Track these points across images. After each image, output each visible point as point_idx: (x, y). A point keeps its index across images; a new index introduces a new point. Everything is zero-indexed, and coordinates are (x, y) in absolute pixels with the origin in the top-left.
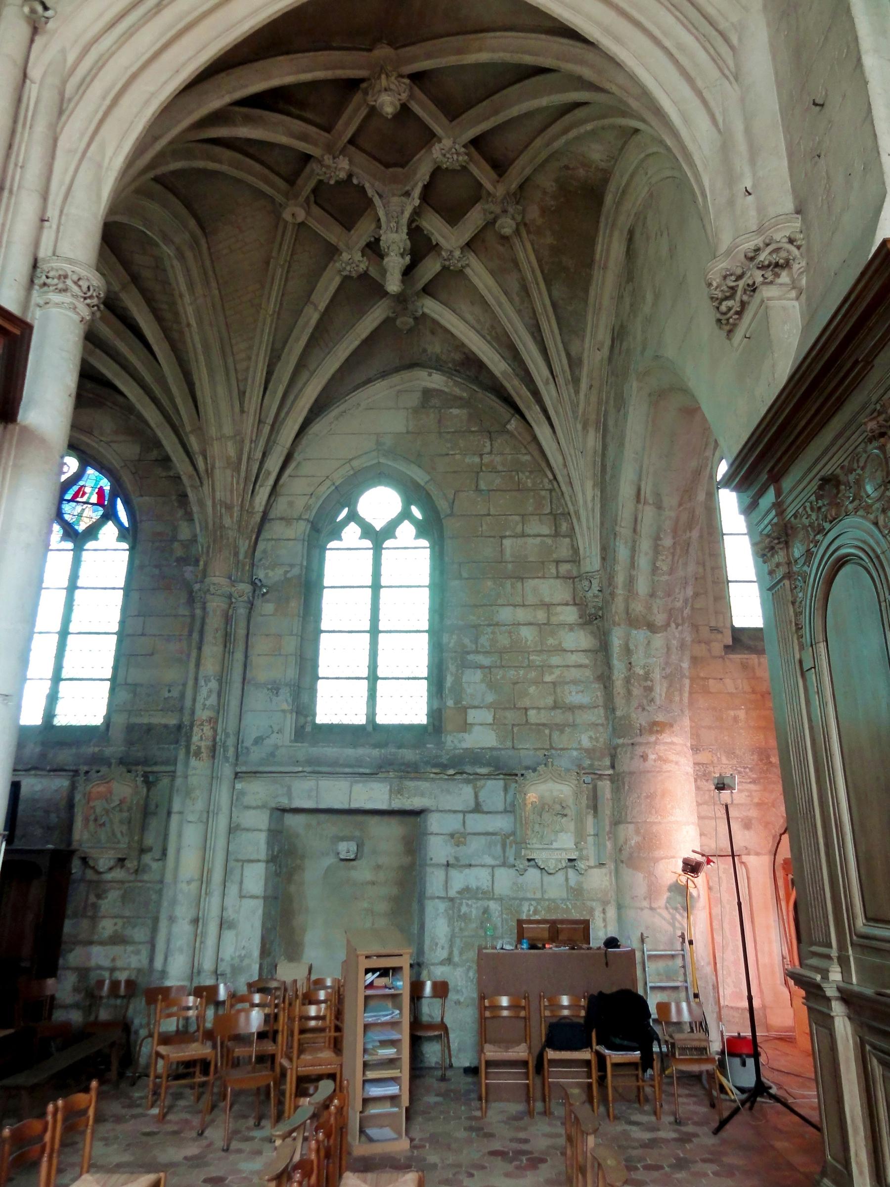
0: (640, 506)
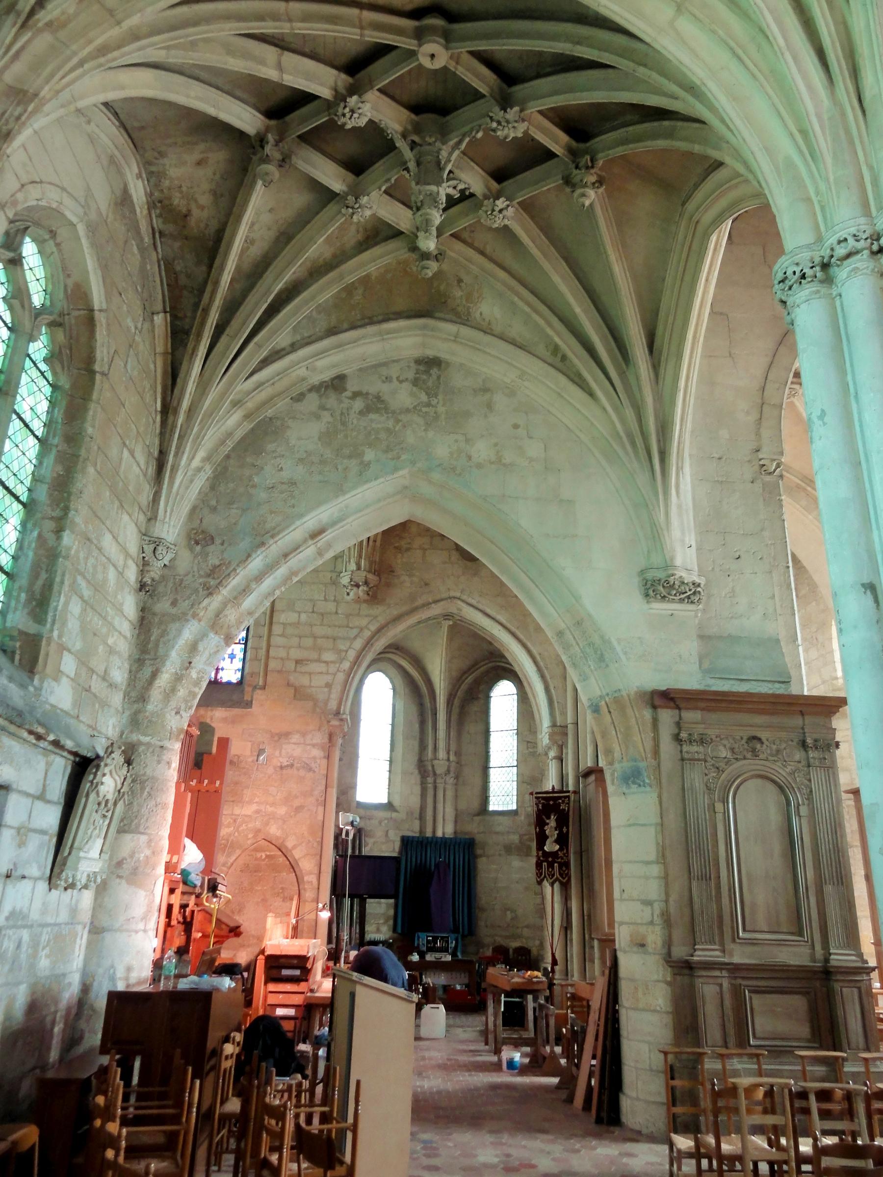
0: (310, 542)
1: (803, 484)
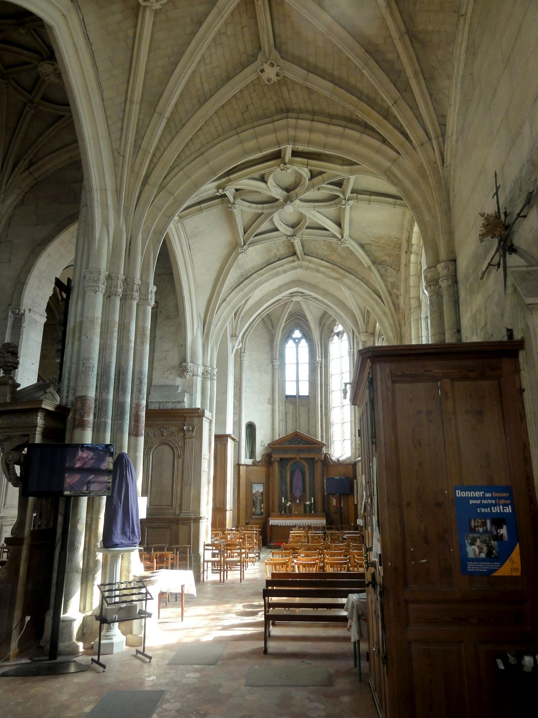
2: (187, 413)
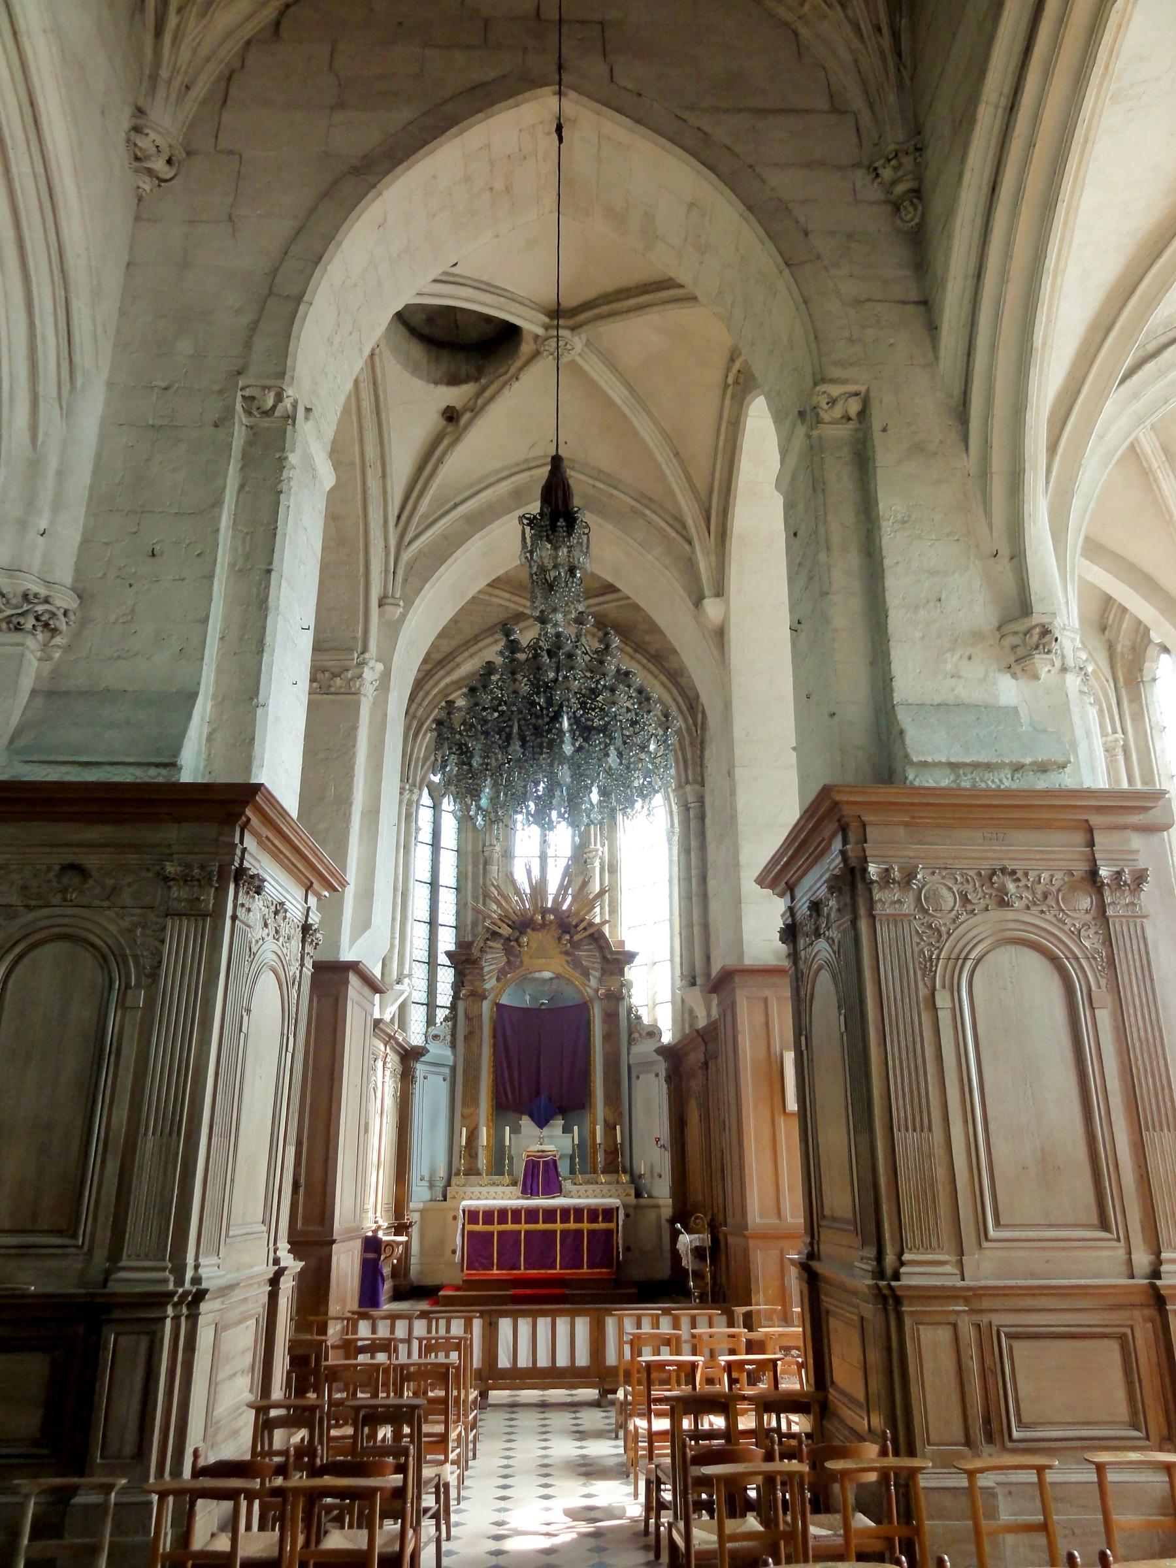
1: (638, 506)
2: (1099, 809)
